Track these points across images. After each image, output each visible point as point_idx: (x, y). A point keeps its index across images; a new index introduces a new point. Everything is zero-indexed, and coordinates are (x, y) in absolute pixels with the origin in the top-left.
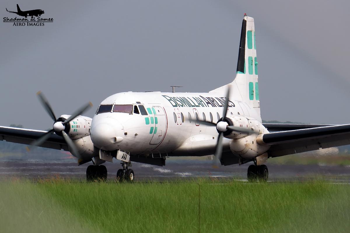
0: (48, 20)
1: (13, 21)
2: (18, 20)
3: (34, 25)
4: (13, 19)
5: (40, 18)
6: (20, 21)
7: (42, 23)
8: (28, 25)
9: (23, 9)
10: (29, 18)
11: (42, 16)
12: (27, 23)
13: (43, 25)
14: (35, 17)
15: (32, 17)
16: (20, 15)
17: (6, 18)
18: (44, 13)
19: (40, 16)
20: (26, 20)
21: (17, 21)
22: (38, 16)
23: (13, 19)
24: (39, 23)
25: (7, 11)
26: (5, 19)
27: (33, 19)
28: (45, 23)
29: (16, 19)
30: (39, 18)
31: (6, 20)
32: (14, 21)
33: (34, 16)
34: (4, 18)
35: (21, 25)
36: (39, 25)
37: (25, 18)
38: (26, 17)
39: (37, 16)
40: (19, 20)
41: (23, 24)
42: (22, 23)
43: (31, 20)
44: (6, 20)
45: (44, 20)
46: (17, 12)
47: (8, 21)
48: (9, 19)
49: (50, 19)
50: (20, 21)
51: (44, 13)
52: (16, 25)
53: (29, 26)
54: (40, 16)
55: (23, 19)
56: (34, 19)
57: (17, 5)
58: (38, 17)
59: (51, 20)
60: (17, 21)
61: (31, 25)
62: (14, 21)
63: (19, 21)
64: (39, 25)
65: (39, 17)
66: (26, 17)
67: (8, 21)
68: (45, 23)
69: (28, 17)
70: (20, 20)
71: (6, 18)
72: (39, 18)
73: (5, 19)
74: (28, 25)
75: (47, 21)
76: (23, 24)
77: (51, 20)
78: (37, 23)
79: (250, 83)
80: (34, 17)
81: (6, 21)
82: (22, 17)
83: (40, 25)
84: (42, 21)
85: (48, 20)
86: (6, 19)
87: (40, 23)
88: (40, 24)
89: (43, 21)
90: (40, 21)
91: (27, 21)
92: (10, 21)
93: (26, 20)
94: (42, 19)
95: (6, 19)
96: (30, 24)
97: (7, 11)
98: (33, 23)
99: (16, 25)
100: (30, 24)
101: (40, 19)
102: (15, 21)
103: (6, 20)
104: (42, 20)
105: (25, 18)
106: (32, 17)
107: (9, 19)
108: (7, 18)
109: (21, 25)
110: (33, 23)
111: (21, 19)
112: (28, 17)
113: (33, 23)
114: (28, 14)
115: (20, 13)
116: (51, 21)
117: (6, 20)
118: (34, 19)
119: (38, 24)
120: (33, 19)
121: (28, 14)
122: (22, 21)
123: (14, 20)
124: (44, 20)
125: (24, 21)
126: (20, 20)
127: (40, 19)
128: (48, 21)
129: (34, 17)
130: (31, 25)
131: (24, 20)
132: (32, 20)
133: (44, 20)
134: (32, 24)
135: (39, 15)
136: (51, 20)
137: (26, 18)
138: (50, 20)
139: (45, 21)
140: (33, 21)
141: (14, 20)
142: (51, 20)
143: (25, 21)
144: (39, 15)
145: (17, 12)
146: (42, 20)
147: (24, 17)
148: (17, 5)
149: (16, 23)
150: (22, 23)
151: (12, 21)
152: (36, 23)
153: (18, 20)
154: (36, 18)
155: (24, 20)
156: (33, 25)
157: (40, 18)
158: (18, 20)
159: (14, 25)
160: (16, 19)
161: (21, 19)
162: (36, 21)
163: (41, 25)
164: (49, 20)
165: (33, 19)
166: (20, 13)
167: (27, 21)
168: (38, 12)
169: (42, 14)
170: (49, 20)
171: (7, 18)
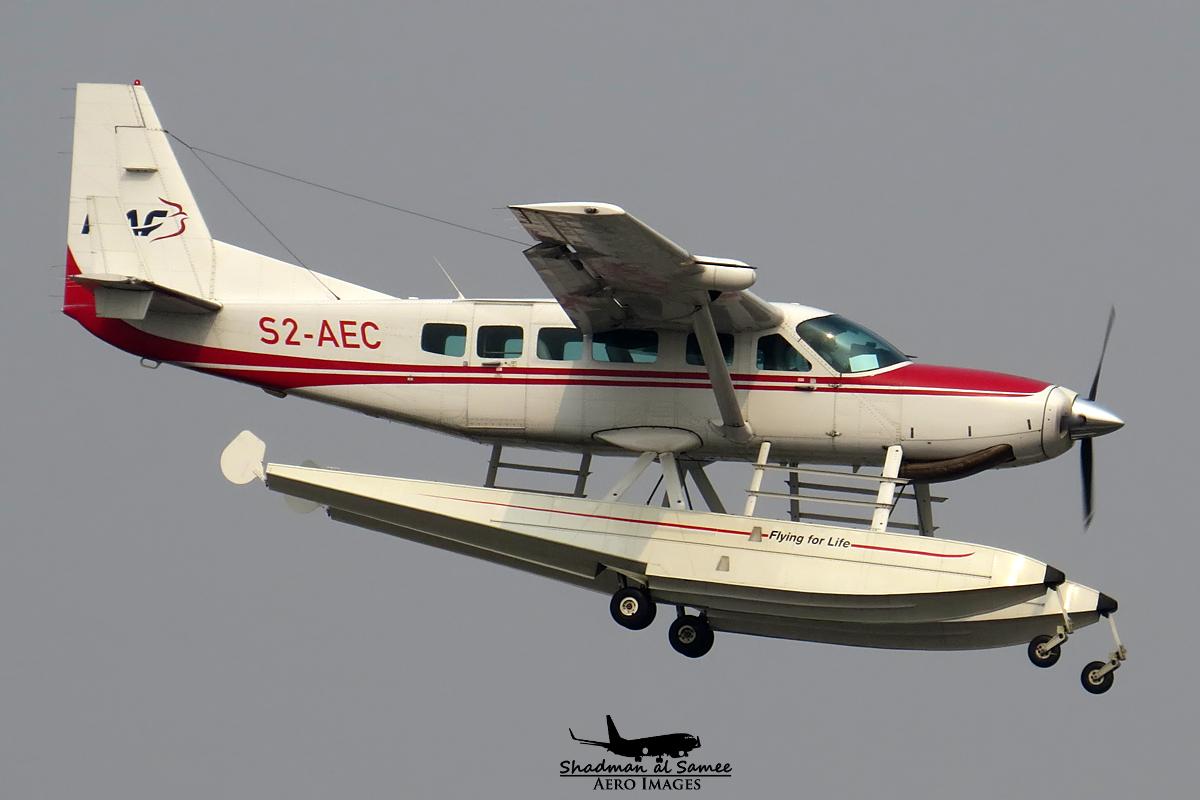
0: (714, 768)
1: (595, 773)
2: (610, 768)
3: (667, 788)
5: (685, 762)
6: (619, 772)
7: (694, 779)
8: (644, 788)
9: (627, 733)
10: (649, 762)
11: (695, 757)
12: (641, 779)
13: (697, 787)
14: (669, 758)
15: (660, 760)
18: (699, 746)
19: (686, 755)
20: (637, 769)
21: (607, 773)
22: (678, 756)
24: (684, 778)
25: (572, 735)
26: (565, 765)
27: (663, 765)
28: (703, 781)
29: (602, 765)
30: (681, 765)
31: (569, 769)
32: (599, 773)
33: (665, 757)
34: (562, 764)
35: (622, 785)
37: (634, 764)
38: (638, 759)
39: (676, 755)
40: (616, 770)
42: (623, 779)
43: (655, 771)
44: (569, 769)
46: (608, 742)
47: (577, 772)
48: (578, 767)
50: (616, 774)
51: (699, 746)
52: (604, 785)
54: (686, 755)
55: (629, 767)
56: (665, 768)
57: (609, 717)
58: (679, 760)
59: (725, 770)
60: (607, 773)
62: (599, 773)
63: (613, 773)
65: (684, 759)
66: (638, 759)
67: (577, 772)
68: (703, 781)
69: (644, 758)
73: (565, 765)
74: (644, 788)
75: (709, 772)
77: (725, 770)
80: (664, 761)
81: (570, 773)
83: (684, 787)
84: (693, 773)
85: (714, 768)
86: (570, 766)
88: (687, 784)
89: (697, 772)
90: (686, 773)
91: (640, 773)
92: (583, 773)
93: (637, 769)
94: (692, 767)
95: (570, 766)
96: (651, 782)
97: (572, 735)
98: (663, 781)
99: (604, 785)
100: (651, 782)
101: (687, 766)
102: (602, 773)
104: (693, 769)
105: (634, 764)
106: (660, 760)
107: (578, 767)
108: (574, 762)
109: (622, 785)
110: (661, 779)
111: (620, 767)
112: (644, 758)
113: (663, 781)
114: (645, 751)
115: (617, 744)
116: (723, 773)
118: (665, 768)
119: (678, 786)
122: (624, 773)
124: (700, 771)
125: (630, 773)
127: (687, 766)
128: (715, 773)
129: (664, 761)
132: (657, 769)
133: (700, 771)
134: (658, 783)
135: (681, 753)
136: (723, 769)
137: (640, 764)
138: (722, 768)
139: (703, 772)
140: (664, 773)
141: (596, 770)
142: (723, 769)
143: (634, 773)
144: (681, 753)
145: (608, 742)
146: (693, 769)
147: (631, 760)
148: (609, 717)
149: (603, 781)
150: (623, 779)
151: (590, 773)
152: (671, 780)
153: (610, 771)
154: (672, 763)
155: (631, 769)
157: (685, 762)
158: (610, 771)
159: (599, 787)
160: (603, 767)
161: (620, 767)
162: (674, 772)
163: (690, 787)
164: (717, 770)
166: (617, 744)
167: (640, 773)
168: (678, 744)
170: (717, 770)
171: (574, 762)
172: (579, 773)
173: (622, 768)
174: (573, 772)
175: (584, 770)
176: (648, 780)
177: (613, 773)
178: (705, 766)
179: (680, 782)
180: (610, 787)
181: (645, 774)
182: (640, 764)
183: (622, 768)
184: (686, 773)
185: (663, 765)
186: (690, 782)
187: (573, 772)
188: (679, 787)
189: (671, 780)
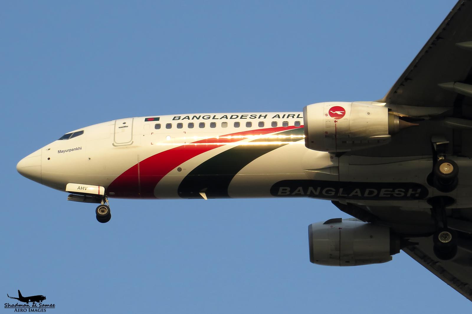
0: (50, 305)
1: (15, 307)
2: (19, 306)
4: (14, 305)
6: (22, 307)
7: (44, 309)
8: (29, 311)
9: (24, 295)
10: (31, 304)
11: (44, 302)
12: (28, 309)
13: (45, 311)
14: (37, 302)
15: (34, 303)
16: (21, 301)
17: (7, 304)
18: (46, 299)
19: (42, 302)
20: (27, 306)
23: (14, 305)
25: (8, 297)
26: (6, 304)
27: (35, 305)
28: (47, 309)
29: (17, 305)
30: (40, 304)
31: (7, 306)
33: (35, 302)
34: (5, 304)
35: (23, 311)
36: (40, 311)
38: (28, 303)
39: (38, 302)
40: (21, 306)
41: (25, 310)
42: (23, 309)
43: (32, 306)
44: (7, 306)
45: (46, 306)
46: (19, 298)
47: (9, 307)
48: (10, 305)
49: (51, 304)
50: (21, 307)
51: (46, 299)
52: (18, 311)
53: (30, 312)
54: (42, 302)
55: (25, 305)
56: (35, 305)
57: (19, 291)
58: (39, 303)
59: (53, 306)
60: (18, 307)
61: (32, 311)
63: (20, 307)
64: (40, 311)
65: (41, 303)
66: (28, 303)
67: (9, 307)
68: (47, 309)
70: (22, 306)
71: (7, 304)
72: (40, 304)
73: (6, 304)
74: (29, 311)
75: (48, 307)
76: (25, 310)
77: (53, 306)
78: (38, 308)
79: (316, 257)
81: (7, 307)
82: (23, 303)
84: (44, 307)
85: (50, 305)
86: (7, 305)
87: (42, 309)
88: (42, 310)
89: (45, 307)
90: (42, 307)
91: (28, 307)
92: (11, 307)
93: (27, 306)
94: (43, 305)
95: (7, 305)
96: (31, 310)
97: (8, 297)
98: (35, 309)
99: (18, 311)
100: (31, 310)
101: (42, 305)
102: (17, 307)
103: (7, 306)
106: (34, 303)
107: (10, 305)
109: (23, 311)
111: (22, 305)
112: (29, 303)
113: (35, 309)
114: (30, 300)
115: (21, 298)
116: (53, 307)
117: (7, 306)
118: (35, 305)
119: (39, 311)
120: (35, 305)
121: (30, 300)
122: (23, 307)
123: (15, 306)
125: (25, 307)
126: (22, 306)
127: (42, 305)
128: (50, 307)
130: (32, 311)
131: (25, 306)
134: (33, 310)
135: (40, 301)
136: (53, 306)
139: (47, 307)
140: (35, 307)
141: (15, 306)
142: (53, 306)
143: (26, 307)
144: (40, 301)
145: (19, 298)
147: (25, 303)
148: (19, 291)
149: (17, 309)
150: (23, 309)
151: (13, 307)
152: (37, 309)
153: (19, 306)
154: (37, 304)
155: (25, 306)
156: (34, 311)
158: (21, 306)
159: (16, 311)
160: (17, 305)
162: (38, 307)
163: (43, 311)
164: (51, 306)
165: (35, 305)
166: (21, 298)
167: (28, 307)
169: (44, 300)
170: (51, 306)
172: (11, 307)
173: (23, 305)
174: (8, 306)
175: (12, 306)
176: (30, 309)
177: (20, 307)
178: (47, 305)
179: (40, 310)
180: (19, 311)
181: (30, 307)
182: (28, 304)
183: (23, 305)
184: (42, 307)
185: (35, 305)
186: (43, 310)
187: (8, 306)
188: (39, 311)
189: (37, 309)
